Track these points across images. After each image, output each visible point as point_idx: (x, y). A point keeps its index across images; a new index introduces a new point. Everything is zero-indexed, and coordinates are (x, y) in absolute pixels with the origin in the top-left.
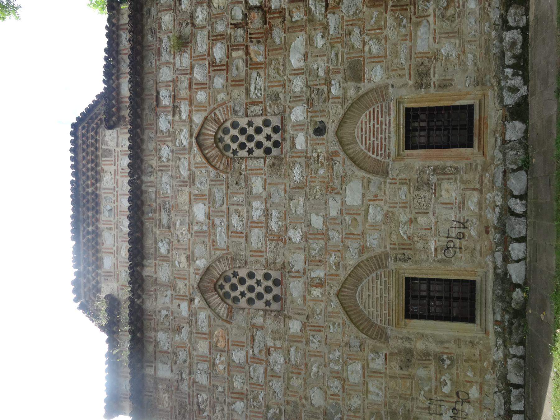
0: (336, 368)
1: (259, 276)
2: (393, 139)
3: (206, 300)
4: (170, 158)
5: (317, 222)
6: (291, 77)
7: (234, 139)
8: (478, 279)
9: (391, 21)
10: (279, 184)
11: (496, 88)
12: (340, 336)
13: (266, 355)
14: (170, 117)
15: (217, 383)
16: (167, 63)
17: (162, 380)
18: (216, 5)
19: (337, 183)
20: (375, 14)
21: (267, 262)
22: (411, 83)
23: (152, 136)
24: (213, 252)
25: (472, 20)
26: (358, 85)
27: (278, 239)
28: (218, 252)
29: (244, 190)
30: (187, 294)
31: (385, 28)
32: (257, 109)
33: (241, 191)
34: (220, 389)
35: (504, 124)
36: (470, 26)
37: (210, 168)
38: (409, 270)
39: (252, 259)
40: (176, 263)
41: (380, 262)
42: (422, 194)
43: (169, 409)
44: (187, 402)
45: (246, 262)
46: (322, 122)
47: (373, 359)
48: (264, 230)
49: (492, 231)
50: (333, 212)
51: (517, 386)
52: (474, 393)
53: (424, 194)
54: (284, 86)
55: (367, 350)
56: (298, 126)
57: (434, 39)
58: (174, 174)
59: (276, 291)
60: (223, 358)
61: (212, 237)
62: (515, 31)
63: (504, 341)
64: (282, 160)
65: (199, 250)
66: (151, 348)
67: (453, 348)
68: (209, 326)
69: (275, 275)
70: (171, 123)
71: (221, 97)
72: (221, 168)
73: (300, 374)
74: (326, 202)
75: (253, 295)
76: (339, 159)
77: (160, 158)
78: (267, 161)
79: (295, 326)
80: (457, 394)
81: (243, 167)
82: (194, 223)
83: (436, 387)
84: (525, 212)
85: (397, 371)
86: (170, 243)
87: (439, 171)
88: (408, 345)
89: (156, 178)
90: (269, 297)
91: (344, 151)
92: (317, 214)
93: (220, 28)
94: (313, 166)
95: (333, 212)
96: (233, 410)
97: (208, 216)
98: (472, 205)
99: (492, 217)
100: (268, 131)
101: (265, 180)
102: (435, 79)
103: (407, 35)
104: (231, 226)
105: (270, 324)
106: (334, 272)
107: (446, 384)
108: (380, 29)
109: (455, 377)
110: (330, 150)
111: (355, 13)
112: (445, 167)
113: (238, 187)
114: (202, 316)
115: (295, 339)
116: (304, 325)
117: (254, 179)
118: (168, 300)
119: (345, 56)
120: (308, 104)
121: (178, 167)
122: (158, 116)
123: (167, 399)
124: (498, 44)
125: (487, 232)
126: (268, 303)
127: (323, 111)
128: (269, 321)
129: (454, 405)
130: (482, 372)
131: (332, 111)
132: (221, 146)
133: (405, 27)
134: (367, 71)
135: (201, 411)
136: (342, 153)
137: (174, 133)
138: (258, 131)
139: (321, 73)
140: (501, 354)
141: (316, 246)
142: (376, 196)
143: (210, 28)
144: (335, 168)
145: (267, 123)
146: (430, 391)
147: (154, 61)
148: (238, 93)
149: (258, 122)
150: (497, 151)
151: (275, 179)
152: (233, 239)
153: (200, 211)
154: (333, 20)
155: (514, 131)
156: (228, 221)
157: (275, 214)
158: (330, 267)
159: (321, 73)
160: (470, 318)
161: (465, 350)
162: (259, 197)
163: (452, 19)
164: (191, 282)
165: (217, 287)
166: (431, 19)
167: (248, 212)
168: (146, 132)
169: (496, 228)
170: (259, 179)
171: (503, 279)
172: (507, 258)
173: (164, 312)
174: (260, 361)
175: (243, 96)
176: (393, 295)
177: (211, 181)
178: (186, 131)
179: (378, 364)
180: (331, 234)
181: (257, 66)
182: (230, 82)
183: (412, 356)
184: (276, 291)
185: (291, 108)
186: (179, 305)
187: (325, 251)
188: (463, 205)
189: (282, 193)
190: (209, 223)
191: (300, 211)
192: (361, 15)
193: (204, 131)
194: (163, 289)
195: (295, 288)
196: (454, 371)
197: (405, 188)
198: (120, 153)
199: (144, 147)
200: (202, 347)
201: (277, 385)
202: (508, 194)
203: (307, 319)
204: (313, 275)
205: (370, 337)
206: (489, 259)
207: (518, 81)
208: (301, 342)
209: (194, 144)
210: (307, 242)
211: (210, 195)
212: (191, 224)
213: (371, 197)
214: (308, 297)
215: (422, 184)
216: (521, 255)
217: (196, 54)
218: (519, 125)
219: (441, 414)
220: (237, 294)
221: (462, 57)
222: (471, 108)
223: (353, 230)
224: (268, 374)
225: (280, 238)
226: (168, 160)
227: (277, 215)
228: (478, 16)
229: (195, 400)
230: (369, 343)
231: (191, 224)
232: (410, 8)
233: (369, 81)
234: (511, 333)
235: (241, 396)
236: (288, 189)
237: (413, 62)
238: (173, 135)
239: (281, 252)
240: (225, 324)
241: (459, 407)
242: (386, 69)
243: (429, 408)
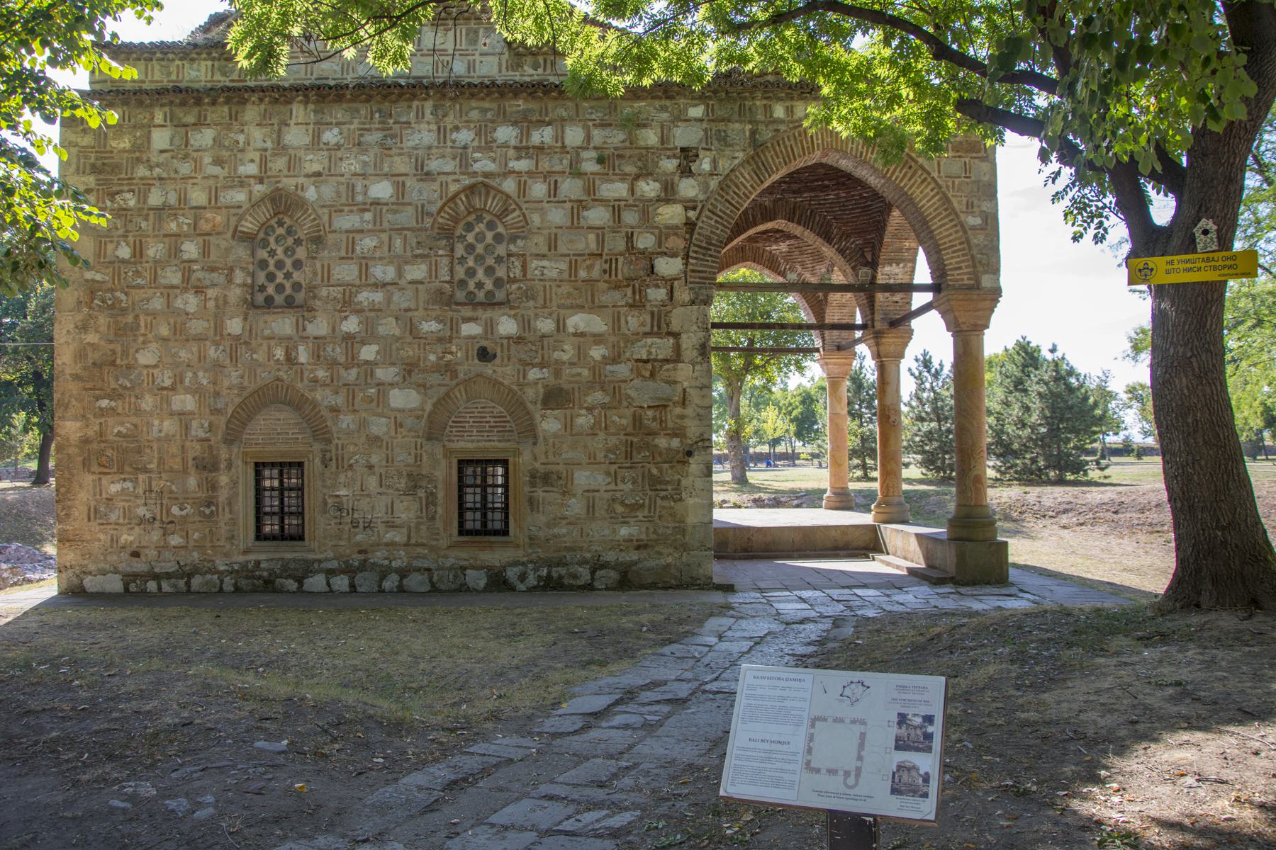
0: (187, 380)
1: (297, 276)
2: (470, 445)
3: (262, 200)
4: (457, 144)
5: (368, 352)
6: (555, 316)
7: (480, 237)
8: (307, 542)
9: (613, 440)
10: (417, 301)
11: (525, 559)
12: (226, 383)
13: (197, 287)
14: (513, 142)
15: (151, 217)
16: (588, 138)
17: (148, 137)
18: (660, 210)
19: (417, 377)
20: (624, 422)
21: (315, 287)
22: (537, 465)
23: (489, 115)
24: (326, 211)
25: (606, 532)
26: (539, 403)
27: (345, 302)
28: (326, 218)
29: (409, 254)
30: (269, 173)
32: (517, 272)
33: (408, 248)
34: (144, 224)
35: (481, 568)
36: (600, 530)
37: (440, 204)
38: (314, 465)
39: (318, 265)
40: (311, 157)
41: (321, 433)
42: (403, 481)
43: (108, 148)
44: (123, 176)
45: (315, 258)
46: (495, 356)
47: (202, 426)
48: (357, 282)
49: (362, 557)
50: (381, 374)
51: (188, 584)
52: (175, 540)
53: (403, 484)
54: (544, 306)
55: (213, 418)
56: (490, 326)
57: (588, 491)
58: (434, 151)
59: (279, 299)
60: (185, 228)
61: (346, 209)
63: (237, 571)
64: (449, 305)
65: (328, 191)
66: (190, 119)
67: (225, 517)
68: (227, 207)
69: (300, 297)
70: (505, 145)
71: (536, 219)
72: (440, 220)
73: (175, 334)
74: (393, 364)
75: (271, 268)
76: (448, 379)
77: (457, 129)
78: (447, 286)
79: (234, 326)
80: (172, 522)
81: (441, 252)
82: (365, 182)
83: (176, 499)
84: (384, 591)
85: (190, 455)
86: (338, 147)
87: (431, 499)
88: (222, 466)
89: (428, 123)
90: (271, 290)
91: (458, 385)
92: (378, 353)
93: (630, 218)
94: (439, 349)
95: (381, 374)
96: (118, 243)
97: (377, 203)
98: (390, 536)
99: (378, 556)
100: (489, 285)
101: (422, 283)
102: (540, 494)
104: (360, 236)
105: (235, 294)
106: (306, 374)
107: (181, 509)
109: (191, 520)
110: (460, 368)
111: (628, 396)
112: (435, 505)
113: (414, 245)
114: (240, 196)
115: (219, 328)
116: (238, 338)
117: (424, 267)
118: (260, 145)
119: (576, 386)
120: (519, 338)
121: (443, 156)
122: (515, 124)
123: (122, 146)
125: (360, 552)
126: (262, 288)
127: (509, 359)
128: (238, 291)
129: (158, 517)
130: (199, 547)
131: (509, 370)
132: (471, 218)
133: (606, 456)
134: (556, 412)
135: (112, 196)
136: (454, 382)
137: (491, 149)
138: (490, 271)
139: (556, 355)
140: (222, 568)
141: (338, 352)
142: (401, 426)
143: (631, 202)
144: (436, 375)
145: (498, 283)
146: (171, 492)
147: (594, 117)
148: (539, 243)
149: (501, 272)
150: (453, 561)
151: (423, 296)
152: (344, 239)
153: (382, 190)
154: (622, 370)
155: (477, 579)
156: (369, 231)
157: (378, 297)
158: (312, 371)
159: (556, 355)
160: (260, 536)
161: (223, 530)
162: (400, 273)
163: (611, 510)
164: (285, 179)
165: (281, 216)
166: (613, 487)
167: (381, 259)
168: (494, 105)
169: (365, 561)
170: (424, 275)
171: (307, 569)
172: (330, 573)
173: (241, 138)
174: (186, 279)
175: (534, 251)
176: (284, 448)
177: (423, 206)
178: (492, 167)
179: (197, 430)
180: (353, 372)
181: (574, 268)
182: (555, 231)
183: (210, 471)
184: (279, 299)
185: (515, 316)
186: (252, 161)
187: (332, 364)
188: (390, 525)
189: (405, 305)
190: (365, 204)
191: (382, 330)
192: (625, 403)
193: (492, 193)
194: (274, 136)
195: (284, 325)
196: (197, 518)
197: (411, 460)
198: (471, 58)
199: (474, 103)
200: (198, 197)
201: (157, 304)
202: (403, 573)
203: (246, 343)
204: (301, 348)
205: (229, 421)
206: (330, 554)
207: (532, 580)
208: (215, 335)
209: (473, 180)
210: (344, 339)
211: (404, 204)
212: (364, 176)
213: (399, 420)
214: (272, 343)
215: (415, 482)
216: (335, 588)
217: (597, 182)
218: (482, 583)
219: (146, 504)
220: (273, 245)
221: (564, 522)
222: (505, 532)
223: (358, 399)
224: (170, 291)
225: (347, 305)
226: (454, 142)
227: (377, 300)
229: (126, 188)
230: (221, 421)
231: (364, 176)
233: (543, 416)
234: (247, 578)
235: (138, 252)
236: (410, 314)
237: (561, 468)
238: (489, 146)
239: (329, 306)
240: (231, 230)
241: (157, 524)
242: (555, 436)
243: (151, 491)
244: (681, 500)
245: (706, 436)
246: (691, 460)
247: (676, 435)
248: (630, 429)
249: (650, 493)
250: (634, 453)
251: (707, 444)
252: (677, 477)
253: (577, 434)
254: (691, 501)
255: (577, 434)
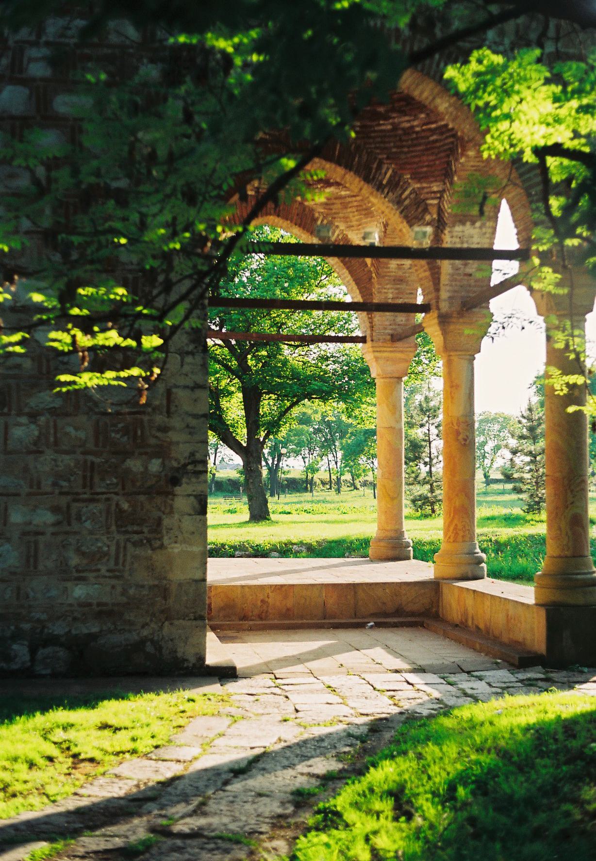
20: (82, 435)
25: (54, 593)
31: (56, 452)
62: (27, 658)
103: (39, 487)
108: (56, 443)
124: (8, 634)
133: (55, 484)
228: (59, 601)
232: (85, 493)
244: (162, 547)
245: (198, 456)
246: (178, 490)
247: (156, 455)
248: (90, 445)
249: (118, 537)
250: (96, 479)
251: (200, 468)
252: (156, 514)
253: (10, 453)
254: (177, 549)
255: (10, 453)
